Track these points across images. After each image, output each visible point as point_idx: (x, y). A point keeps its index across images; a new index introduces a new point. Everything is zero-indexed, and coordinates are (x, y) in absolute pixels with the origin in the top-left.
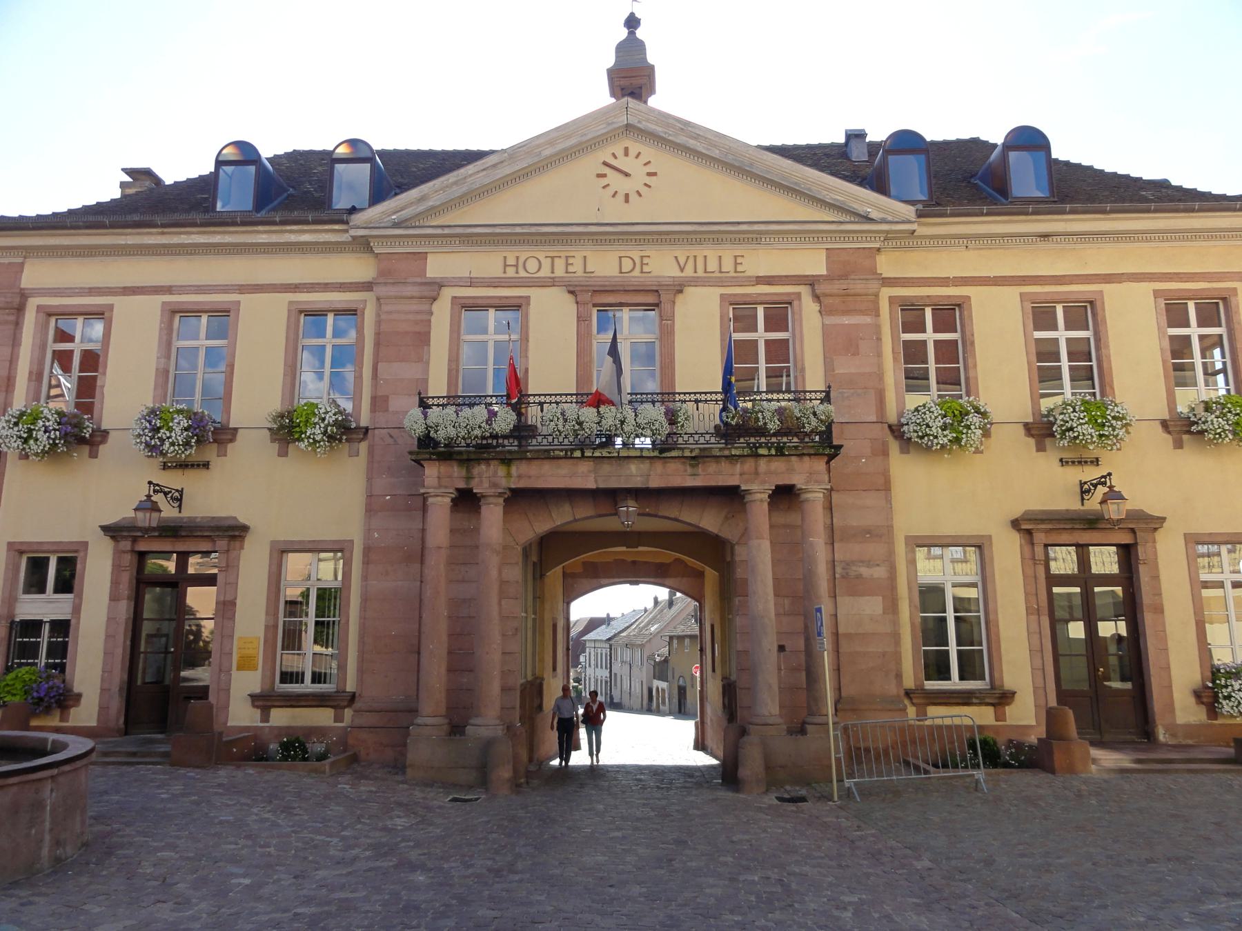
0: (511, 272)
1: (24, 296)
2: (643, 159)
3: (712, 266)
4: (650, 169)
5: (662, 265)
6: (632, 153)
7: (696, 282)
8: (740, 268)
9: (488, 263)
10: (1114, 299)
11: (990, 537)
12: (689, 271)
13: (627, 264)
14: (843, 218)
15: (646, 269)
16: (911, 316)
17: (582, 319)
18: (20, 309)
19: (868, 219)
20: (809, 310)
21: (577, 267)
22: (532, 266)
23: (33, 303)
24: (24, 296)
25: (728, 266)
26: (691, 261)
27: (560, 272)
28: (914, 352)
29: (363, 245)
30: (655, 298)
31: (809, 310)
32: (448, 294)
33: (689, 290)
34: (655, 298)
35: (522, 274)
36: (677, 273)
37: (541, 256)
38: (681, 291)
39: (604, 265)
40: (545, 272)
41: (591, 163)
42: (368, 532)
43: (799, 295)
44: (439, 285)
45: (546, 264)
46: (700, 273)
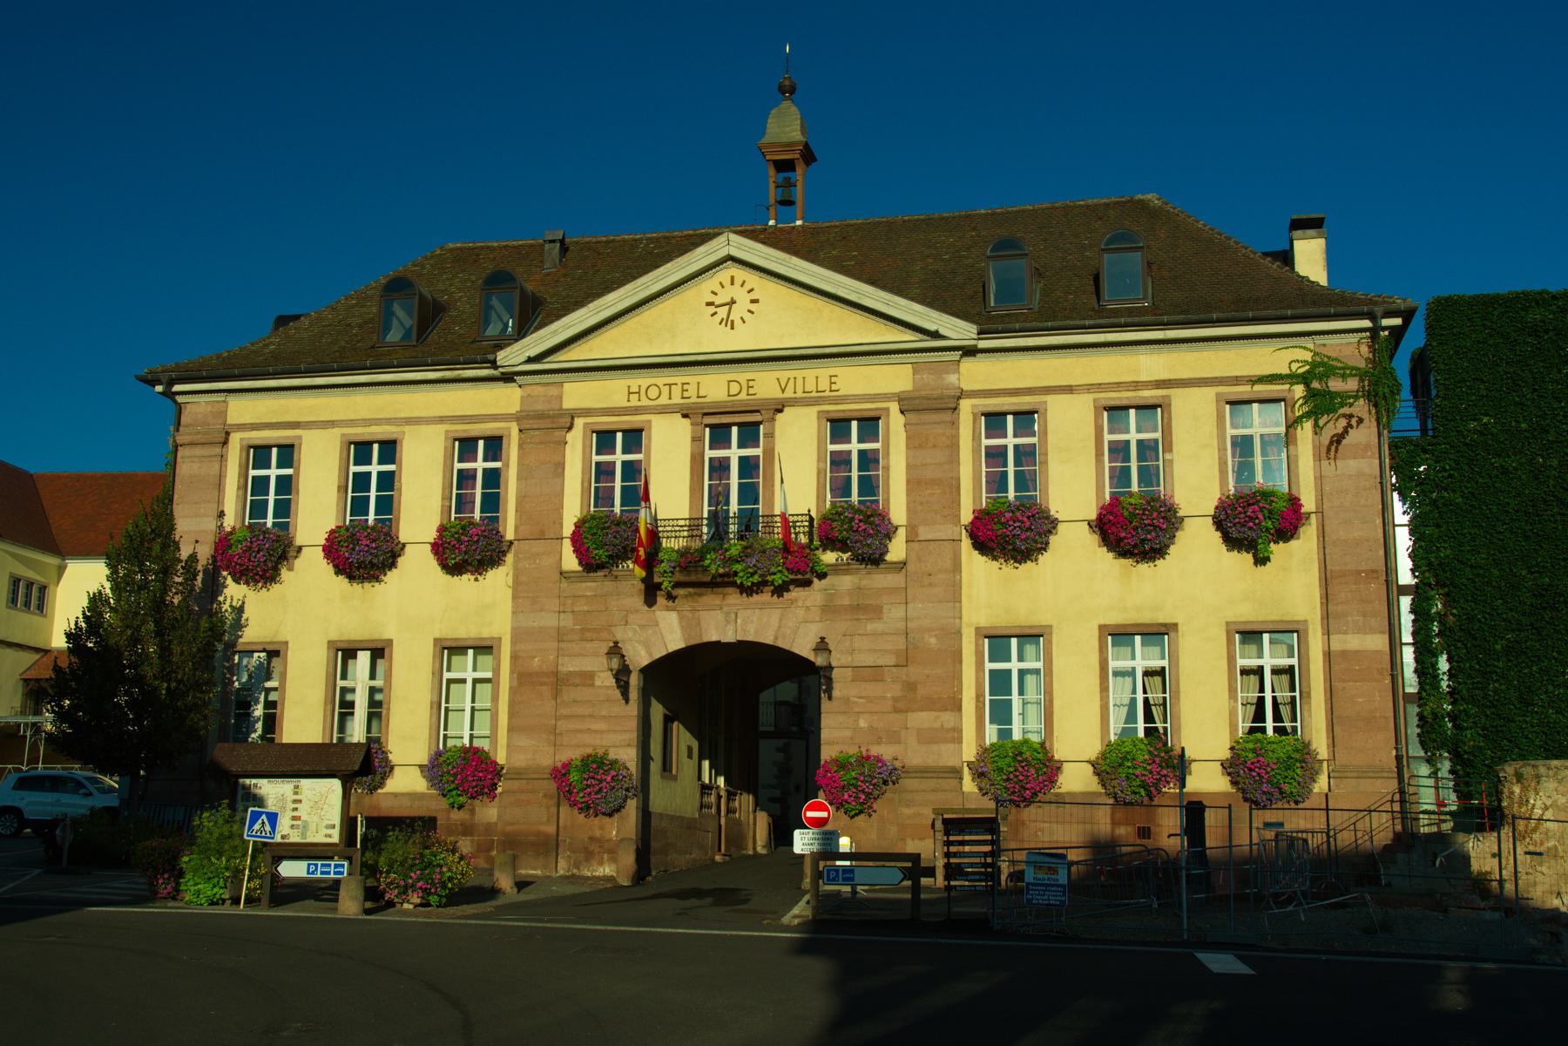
0: (634, 402)
4: (753, 296)
5: (766, 384)
6: (738, 282)
7: (794, 402)
12: (789, 394)
14: (921, 336)
16: (995, 421)
17: (697, 439)
18: (225, 443)
20: (896, 425)
21: (692, 392)
22: (653, 393)
23: (236, 439)
25: (824, 385)
27: (677, 400)
28: (995, 455)
29: (508, 378)
31: (896, 425)
32: (579, 423)
35: (645, 402)
36: (779, 395)
37: (661, 381)
38: (781, 411)
39: (715, 387)
40: (664, 400)
42: (518, 635)
43: (887, 409)
44: (573, 415)
45: (665, 390)
46: (800, 394)
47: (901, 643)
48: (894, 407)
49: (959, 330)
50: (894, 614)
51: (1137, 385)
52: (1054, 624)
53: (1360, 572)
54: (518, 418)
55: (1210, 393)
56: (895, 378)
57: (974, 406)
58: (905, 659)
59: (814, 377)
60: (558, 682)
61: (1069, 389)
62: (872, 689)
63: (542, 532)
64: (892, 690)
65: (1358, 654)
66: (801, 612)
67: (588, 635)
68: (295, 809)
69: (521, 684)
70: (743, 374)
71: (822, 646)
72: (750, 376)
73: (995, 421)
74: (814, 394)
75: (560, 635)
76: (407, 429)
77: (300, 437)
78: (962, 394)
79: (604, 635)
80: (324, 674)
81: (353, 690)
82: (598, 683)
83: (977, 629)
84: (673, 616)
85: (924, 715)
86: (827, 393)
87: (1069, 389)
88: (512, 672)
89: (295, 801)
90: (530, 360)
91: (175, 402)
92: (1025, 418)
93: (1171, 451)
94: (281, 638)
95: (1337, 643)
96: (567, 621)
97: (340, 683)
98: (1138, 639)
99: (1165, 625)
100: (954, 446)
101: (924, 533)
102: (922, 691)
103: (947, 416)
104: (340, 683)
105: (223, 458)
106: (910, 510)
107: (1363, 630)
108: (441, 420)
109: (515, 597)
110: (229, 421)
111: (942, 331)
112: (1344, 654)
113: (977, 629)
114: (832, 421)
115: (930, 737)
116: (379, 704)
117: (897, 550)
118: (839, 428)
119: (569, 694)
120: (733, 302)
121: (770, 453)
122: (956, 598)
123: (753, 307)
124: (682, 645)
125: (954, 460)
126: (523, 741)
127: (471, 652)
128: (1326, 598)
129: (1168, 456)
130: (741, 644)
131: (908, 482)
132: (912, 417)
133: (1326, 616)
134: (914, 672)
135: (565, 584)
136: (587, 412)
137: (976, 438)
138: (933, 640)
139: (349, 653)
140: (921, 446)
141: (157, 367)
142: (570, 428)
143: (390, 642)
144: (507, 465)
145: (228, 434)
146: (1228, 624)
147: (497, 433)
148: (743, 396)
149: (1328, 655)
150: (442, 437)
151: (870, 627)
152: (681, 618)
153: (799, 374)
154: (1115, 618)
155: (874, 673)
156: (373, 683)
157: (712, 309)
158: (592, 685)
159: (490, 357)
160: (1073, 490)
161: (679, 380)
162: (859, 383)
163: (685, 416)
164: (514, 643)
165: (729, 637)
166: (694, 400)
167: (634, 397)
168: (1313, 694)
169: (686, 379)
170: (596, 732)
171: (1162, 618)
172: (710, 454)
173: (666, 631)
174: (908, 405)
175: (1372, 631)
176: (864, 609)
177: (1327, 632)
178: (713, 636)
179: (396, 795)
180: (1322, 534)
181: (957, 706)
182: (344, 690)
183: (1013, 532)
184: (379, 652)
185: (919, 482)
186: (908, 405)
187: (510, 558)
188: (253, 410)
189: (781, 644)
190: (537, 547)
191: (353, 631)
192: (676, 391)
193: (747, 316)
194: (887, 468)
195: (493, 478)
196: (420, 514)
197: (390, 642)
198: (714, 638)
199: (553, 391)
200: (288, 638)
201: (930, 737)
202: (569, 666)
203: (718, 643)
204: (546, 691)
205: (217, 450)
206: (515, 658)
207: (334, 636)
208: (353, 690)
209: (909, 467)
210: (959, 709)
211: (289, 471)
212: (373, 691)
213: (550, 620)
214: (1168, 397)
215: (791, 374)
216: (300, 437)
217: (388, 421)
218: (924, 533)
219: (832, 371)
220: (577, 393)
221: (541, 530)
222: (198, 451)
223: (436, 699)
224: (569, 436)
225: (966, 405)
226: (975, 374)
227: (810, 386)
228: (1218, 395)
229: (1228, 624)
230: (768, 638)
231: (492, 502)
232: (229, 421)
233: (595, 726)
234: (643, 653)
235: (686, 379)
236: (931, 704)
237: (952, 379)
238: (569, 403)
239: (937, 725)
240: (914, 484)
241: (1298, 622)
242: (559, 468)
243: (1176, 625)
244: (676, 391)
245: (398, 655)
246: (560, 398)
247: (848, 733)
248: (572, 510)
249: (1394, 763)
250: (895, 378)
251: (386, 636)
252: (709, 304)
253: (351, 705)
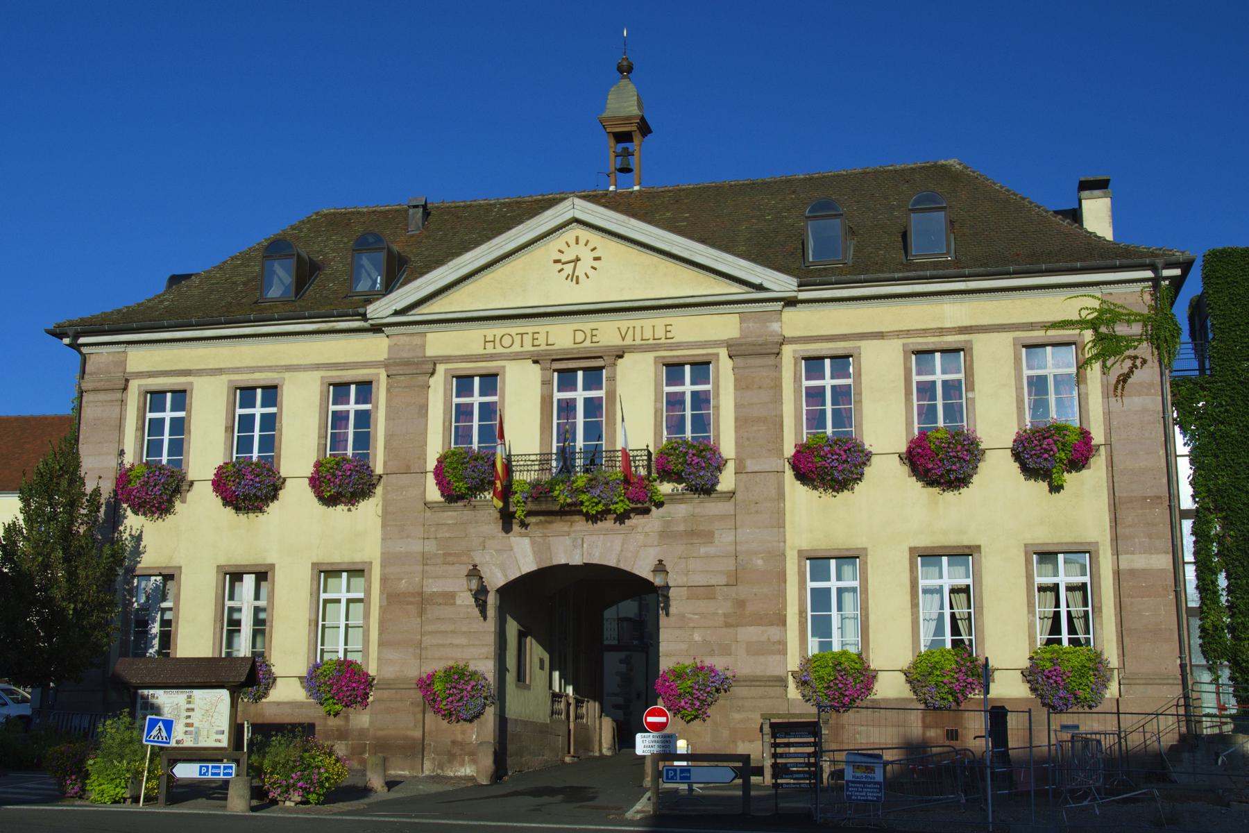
2: (591, 246)
5: (608, 332)
6: (582, 241)
7: (633, 349)
8: (669, 335)
9: (470, 341)
10: (980, 343)
11: (865, 549)
12: (628, 341)
14: (746, 289)
15: (595, 339)
16: (813, 364)
17: (546, 383)
18: (125, 389)
19: (767, 290)
20: (725, 368)
21: (541, 340)
23: (134, 385)
25: (660, 333)
26: (631, 330)
27: (528, 347)
28: (815, 395)
29: (377, 329)
31: (725, 368)
32: (441, 369)
33: (626, 355)
35: (499, 350)
37: (513, 331)
38: (621, 357)
39: (562, 336)
40: (516, 348)
42: (387, 559)
43: (717, 355)
46: (638, 342)
47: (730, 565)
48: (723, 353)
49: (781, 283)
50: (724, 539)
51: (942, 331)
52: (869, 547)
53: (1146, 498)
54: (386, 365)
55: (1008, 337)
56: (725, 326)
57: (795, 351)
58: (735, 579)
59: (652, 326)
60: (423, 601)
61: (880, 335)
62: (704, 606)
63: (408, 467)
64: (723, 607)
65: (1146, 572)
66: (640, 538)
67: (450, 559)
68: (189, 717)
69: (389, 603)
70: (587, 324)
71: (660, 568)
72: (593, 325)
73: (813, 364)
74: (651, 342)
75: (425, 559)
76: (287, 375)
78: (784, 341)
79: (464, 559)
80: (213, 596)
81: (239, 610)
82: (459, 602)
83: (800, 552)
84: (527, 541)
85: (751, 629)
86: (663, 341)
87: (880, 335)
88: (382, 593)
89: (188, 710)
90: (396, 313)
91: (81, 353)
92: (841, 361)
93: (973, 390)
94: (174, 563)
95: (1126, 562)
96: (431, 547)
97: (228, 603)
98: (945, 559)
99: (969, 547)
100: (777, 387)
101: (751, 465)
102: (750, 608)
103: (770, 360)
104: (228, 603)
105: (123, 402)
106: (739, 445)
107: (1150, 550)
108: (317, 367)
109: (384, 525)
110: (129, 369)
111: (766, 285)
112: (1132, 572)
113: (800, 552)
114: (667, 365)
115: (757, 650)
116: (263, 622)
117: (727, 481)
118: (673, 370)
119: (433, 612)
120: (578, 259)
121: (612, 395)
122: (779, 523)
123: (596, 264)
125: (778, 399)
126: (392, 655)
127: (345, 575)
128: (1115, 522)
129: (970, 395)
130: (587, 567)
131: (736, 419)
132: (739, 360)
133: (1115, 539)
134: (743, 591)
135: (428, 513)
136: (447, 359)
137: (797, 380)
138: (760, 562)
139: (236, 577)
140: (747, 388)
141: (62, 319)
142: (432, 374)
143: (272, 566)
144: (376, 407)
145: (127, 381)
146: (1026, 545)
147: (367, 379)
148: (587, 344)
149: (1117, 574)
150: (319, 383)
151: (703, 550)
152: (533, 543)
153: (638, 324)
154: (924, 541)
155: (708, 592)
156: (258, 603)
157: (559, 266)
158: (454, 604)
159: (361, 310)
160: (885, 426)
161: (530, 330)
162: (691, 330)
163: (536, 362)
164: (384, 565)
165: (576, 560)
166: (543, 347)
167: (490, 345)
168: (1104, 608)
169: (536, 329)
170: (457, 646)
171: (966, 540)
172: (558, 395)
173: (521, 555)
174: (736, 350)
175: (1157, 551)
176: (697, 534)
177: (1116, 553)
178: (562, 559)
179: (278, 704)
180: (1111, 464)
181: (783, 622)
182: (232, 610)
183: (831, 464)
184: (262, 576)
186: (736, 350)
187: (379, 490)
188: (150, 360)
189: (623, 566)
190: (405, 480)
191: (240, 556)
193: (591, 272)
194: (717, 408)
195: (364, 419)
196: (299, 452)
197: (272, 566)
198: (563, 561)
199: (417, 340)
200: (182, 563)
201: (757, 650)
202: (433, 587)
203: (567, 565)
204: (413, 609)
205: (118, 395)
206: (384, 580)
207: (222, 561)
208: (239, 610)
209: (738, 406)
210: (784, 623)
211: (182, 414)
212: (257, 610)
213: (416, 547)
214: (970, 341)
215: (631, 324)
217: (270, 368)
218: (751, 465)
219: (668, 321)
220: (438, 343)
221: (408, 466)
222: (101, 397)
223: (314, 617)
224: (432, 381)
225: (788, 351)
226: (795, 322)
227: (648, 334)
229: (1026, 545)
231: (363, 440)
232: (129, 369)
233: (457, 641)
234: (499, 575)
235: (536, 329)
237: (775, 326)
238: (431, 352)
239: (764, 638)
240: (742, 422)
241: (1089, 543)
242: (423, 409)
243: (979, 547)
245: (281, 579)
246: (423, 346)
247: (684, 646)
248: (435, 446)
249: (1178, 671)
250: (725, 326)
251: (269, 561)
252: (556, 261)
253: (238, 623)
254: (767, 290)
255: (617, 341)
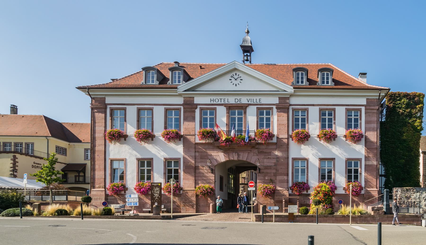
0: (212, 103)
1: (106, 105)
3: (255, 101)
5: (244, 100)
12: (250, 103)
13: (237, 101)
18: (106, 108)
22: (217, 101)
23: (109, 107)
24: (106, 105)
25: (258, 101)
27: (223, 102)
29: (180, 95)
30: (243, 108)
32: (199, 107)
34: (243, 108)
35: (215, 103)
36: (248, 103)
39: (232, 100)
40: (219, 103)
41: (229, 76)
45: (220, 100)
46: (252, 103)
48: (274, 107)
55: (344, 107)
59: (255, 99)
69: (186, 169)
72: (240, 98)
77: (126, 108)
78: (291, 105)
85: (280, 177)
90: (185, 91)
110: (106, 103)
122: (288, 151)
124: (224, 160)
136: (200, 105)
138: (282, 160)
142: (196, 108)
148: (239, 103)
153: (252, 98)
162: (265, 100)
169: (225, 98)
185: (279, 124)
189: (248, 161)
192: (223, 100)
194: (273, 122)
199: (192, 99)
209: (278, 120)
215: (250, 98)
216: (126, 108)
219: (260, 98)
228: (346, 109)
230: (245, 159)
232: (106, 103)
235: (225, 98)
236: (281, 174)
237: (288, 101)
244: (223, 100)
246: (193, 101)
254: (286, 91)
255: (246, 102)
